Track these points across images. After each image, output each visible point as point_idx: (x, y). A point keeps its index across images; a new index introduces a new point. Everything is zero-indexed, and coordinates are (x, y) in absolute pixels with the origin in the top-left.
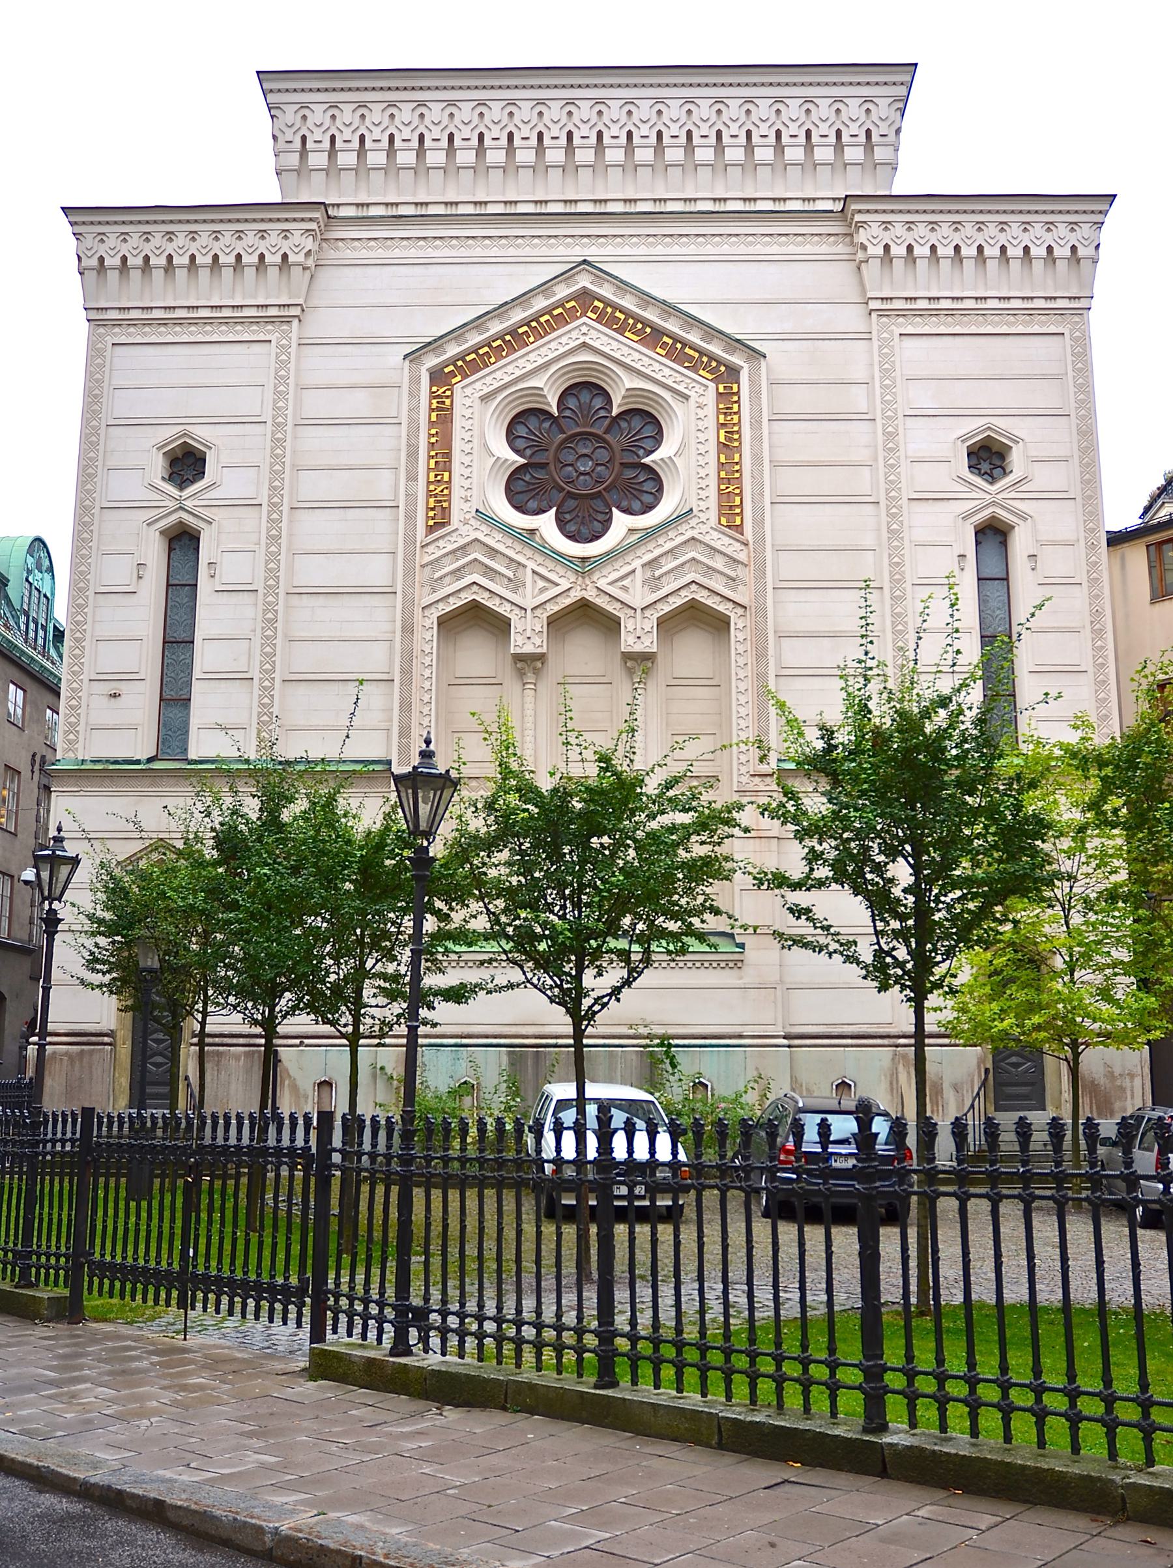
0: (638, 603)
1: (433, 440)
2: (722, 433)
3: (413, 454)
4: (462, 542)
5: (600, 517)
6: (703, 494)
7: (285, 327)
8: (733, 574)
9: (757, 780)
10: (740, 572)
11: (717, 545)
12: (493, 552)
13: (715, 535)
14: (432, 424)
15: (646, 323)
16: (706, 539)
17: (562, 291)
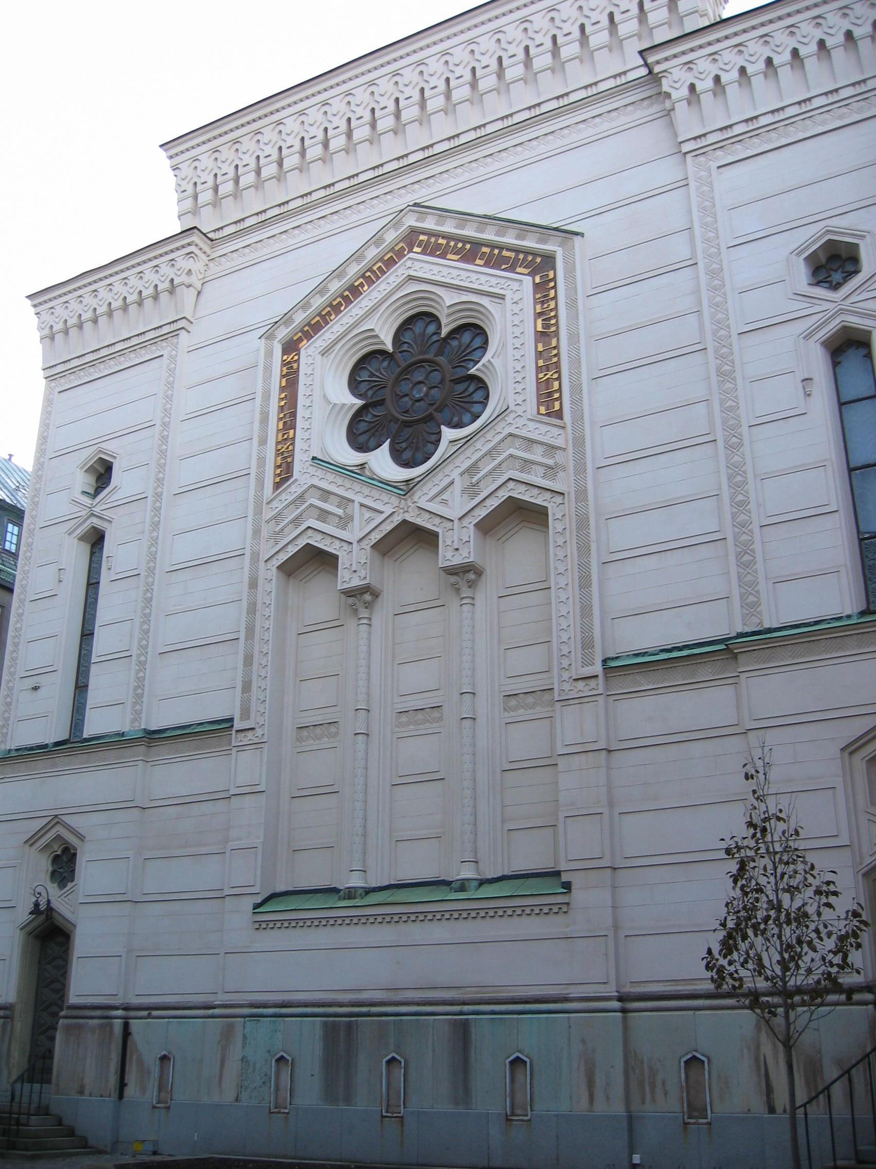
0: (455, 514)
1: (282, 403)
2: (539, 322)
3: (265, 420)
4: (300, 491)
5: (433, 438)
6: (519, 388)
7: (175, 340)
8: (550, 462)
9: (581, 684)
10: (559, 457)
11: (534, 436)
12: (326, 494)
13: (532, 425)
14: (282, 389)
15: (464, 240)
16: (523, 433)
17: (391, 236)
